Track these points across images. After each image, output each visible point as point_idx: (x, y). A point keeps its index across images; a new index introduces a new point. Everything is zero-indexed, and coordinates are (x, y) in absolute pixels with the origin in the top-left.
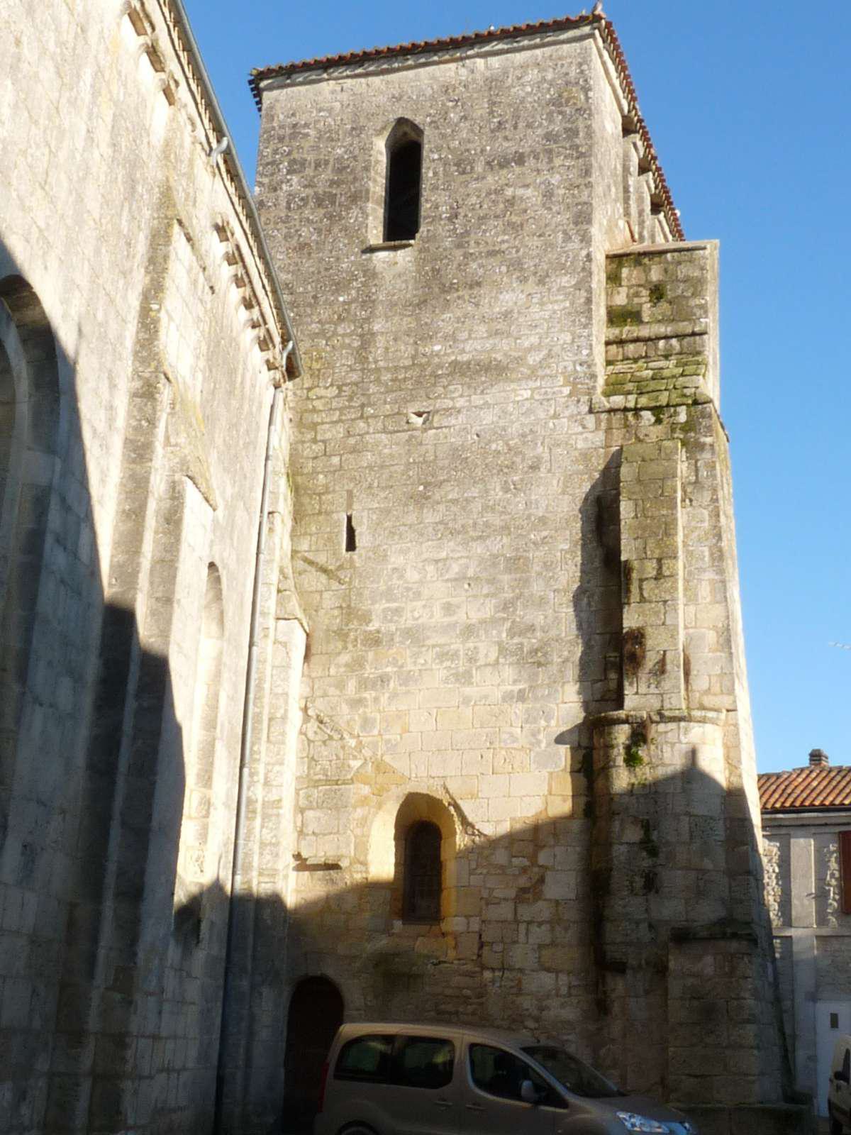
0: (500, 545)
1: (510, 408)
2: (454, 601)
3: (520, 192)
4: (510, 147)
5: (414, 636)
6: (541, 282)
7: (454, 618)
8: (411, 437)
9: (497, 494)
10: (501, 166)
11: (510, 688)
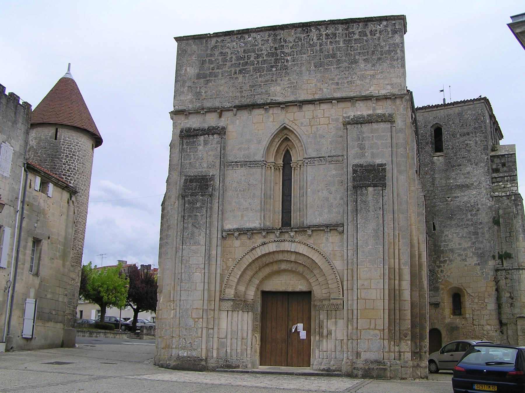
0: (472, 229)
1: (471, 196)
2: (461, 242)
3: (469, 142)
4: (465, 131)
5: (452, 251)
6: (476, 165)
7: (460, 247)
8: (447, 203)
9: (469, 217)
10: (464, 136)
11: (476, 262)
